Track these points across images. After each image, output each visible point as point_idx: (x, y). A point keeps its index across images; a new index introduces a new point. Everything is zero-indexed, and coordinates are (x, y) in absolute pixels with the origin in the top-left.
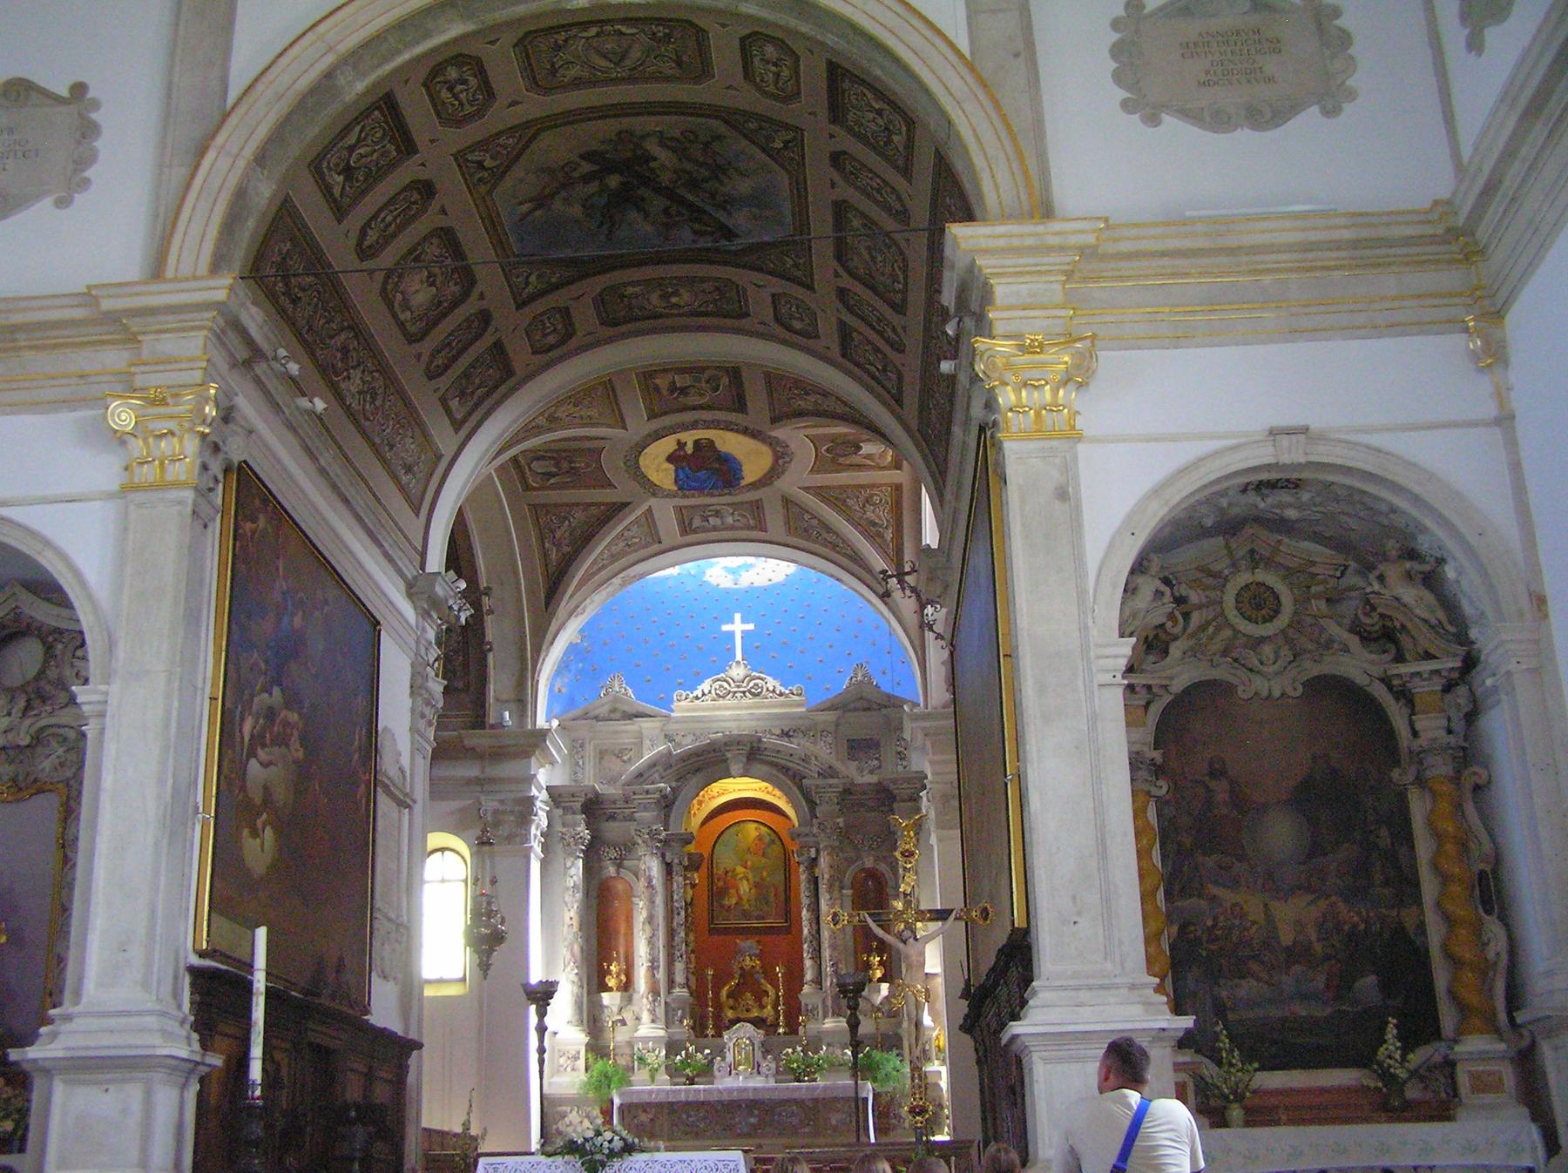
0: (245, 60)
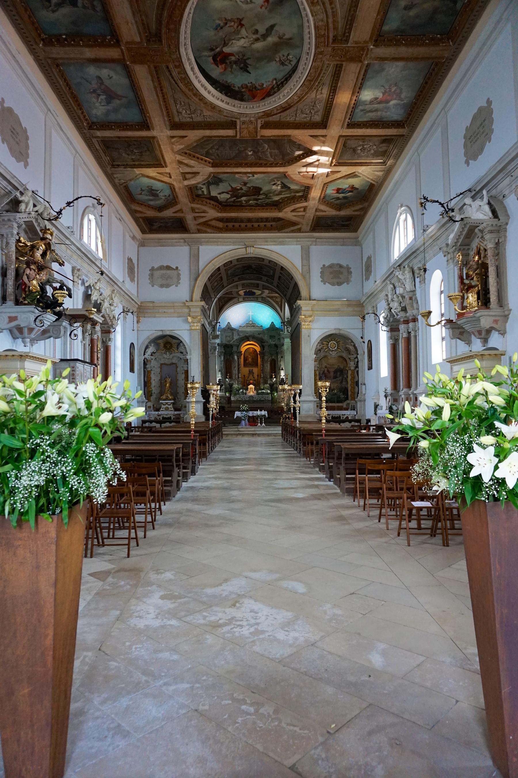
0: (201, 266)
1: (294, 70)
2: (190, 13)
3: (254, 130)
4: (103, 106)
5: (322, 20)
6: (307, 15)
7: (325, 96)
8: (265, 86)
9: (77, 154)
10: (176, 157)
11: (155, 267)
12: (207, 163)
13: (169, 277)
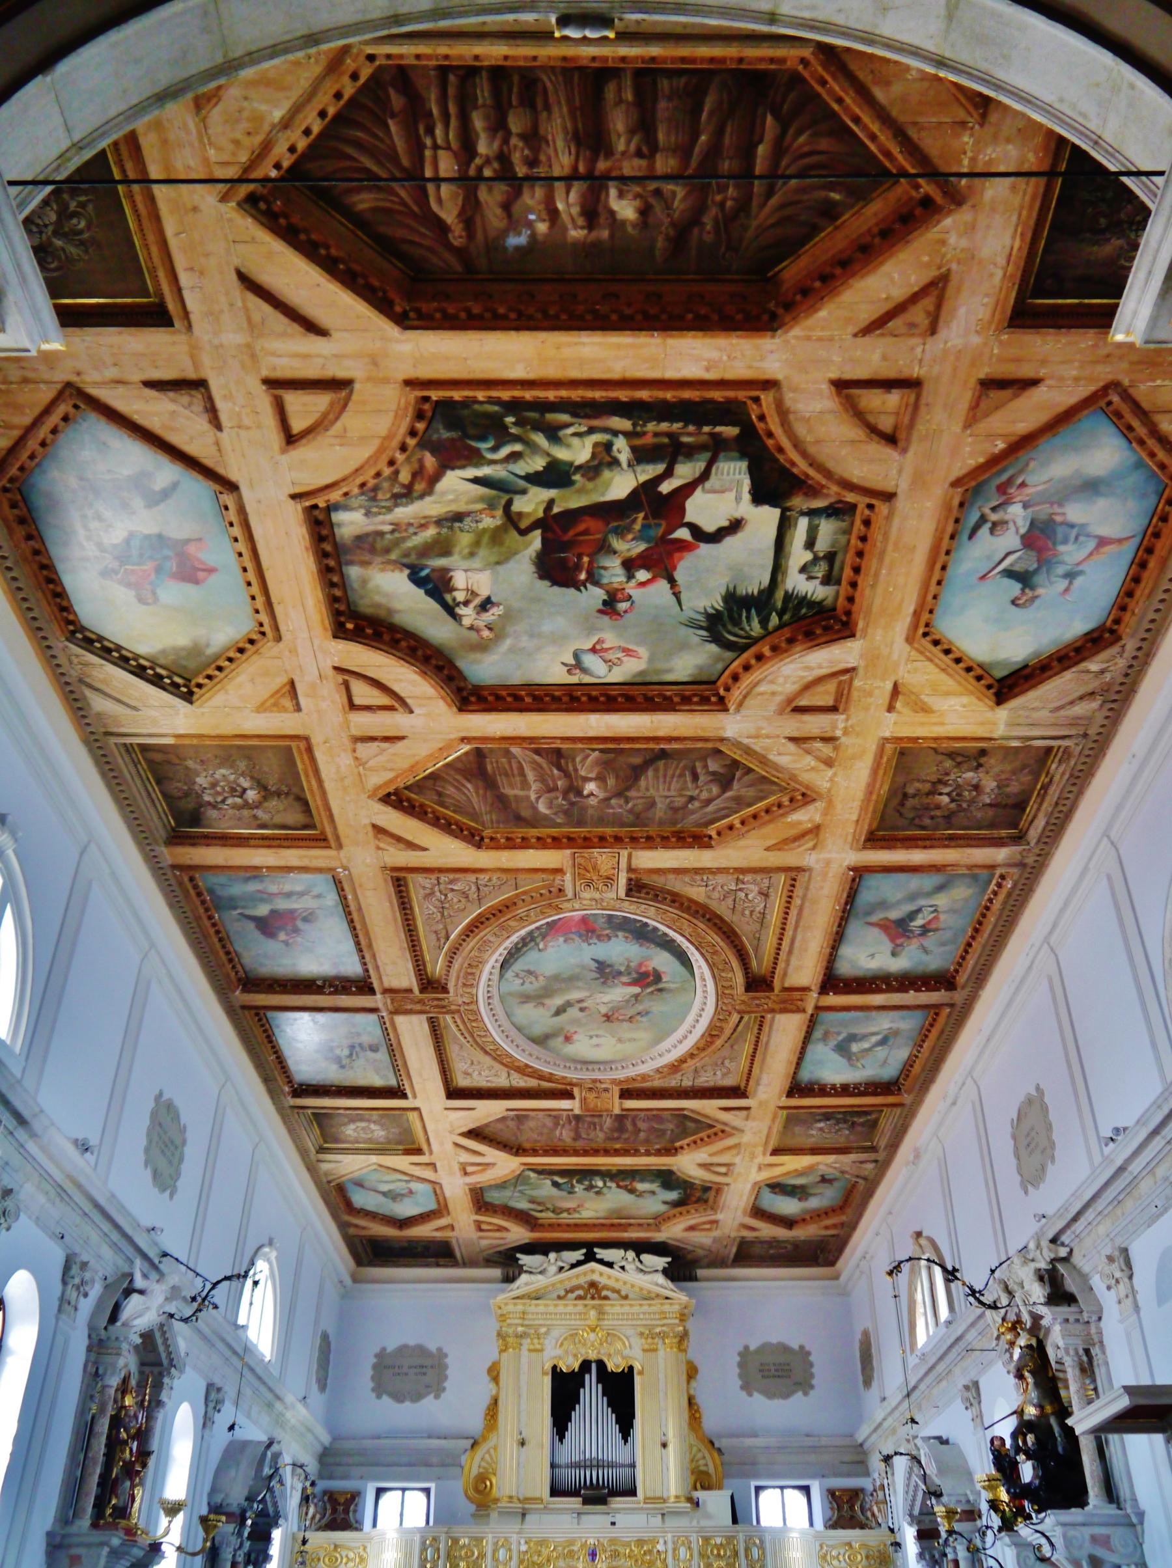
1: (504, 965)
8: (561, 939)
10: (831, 780)
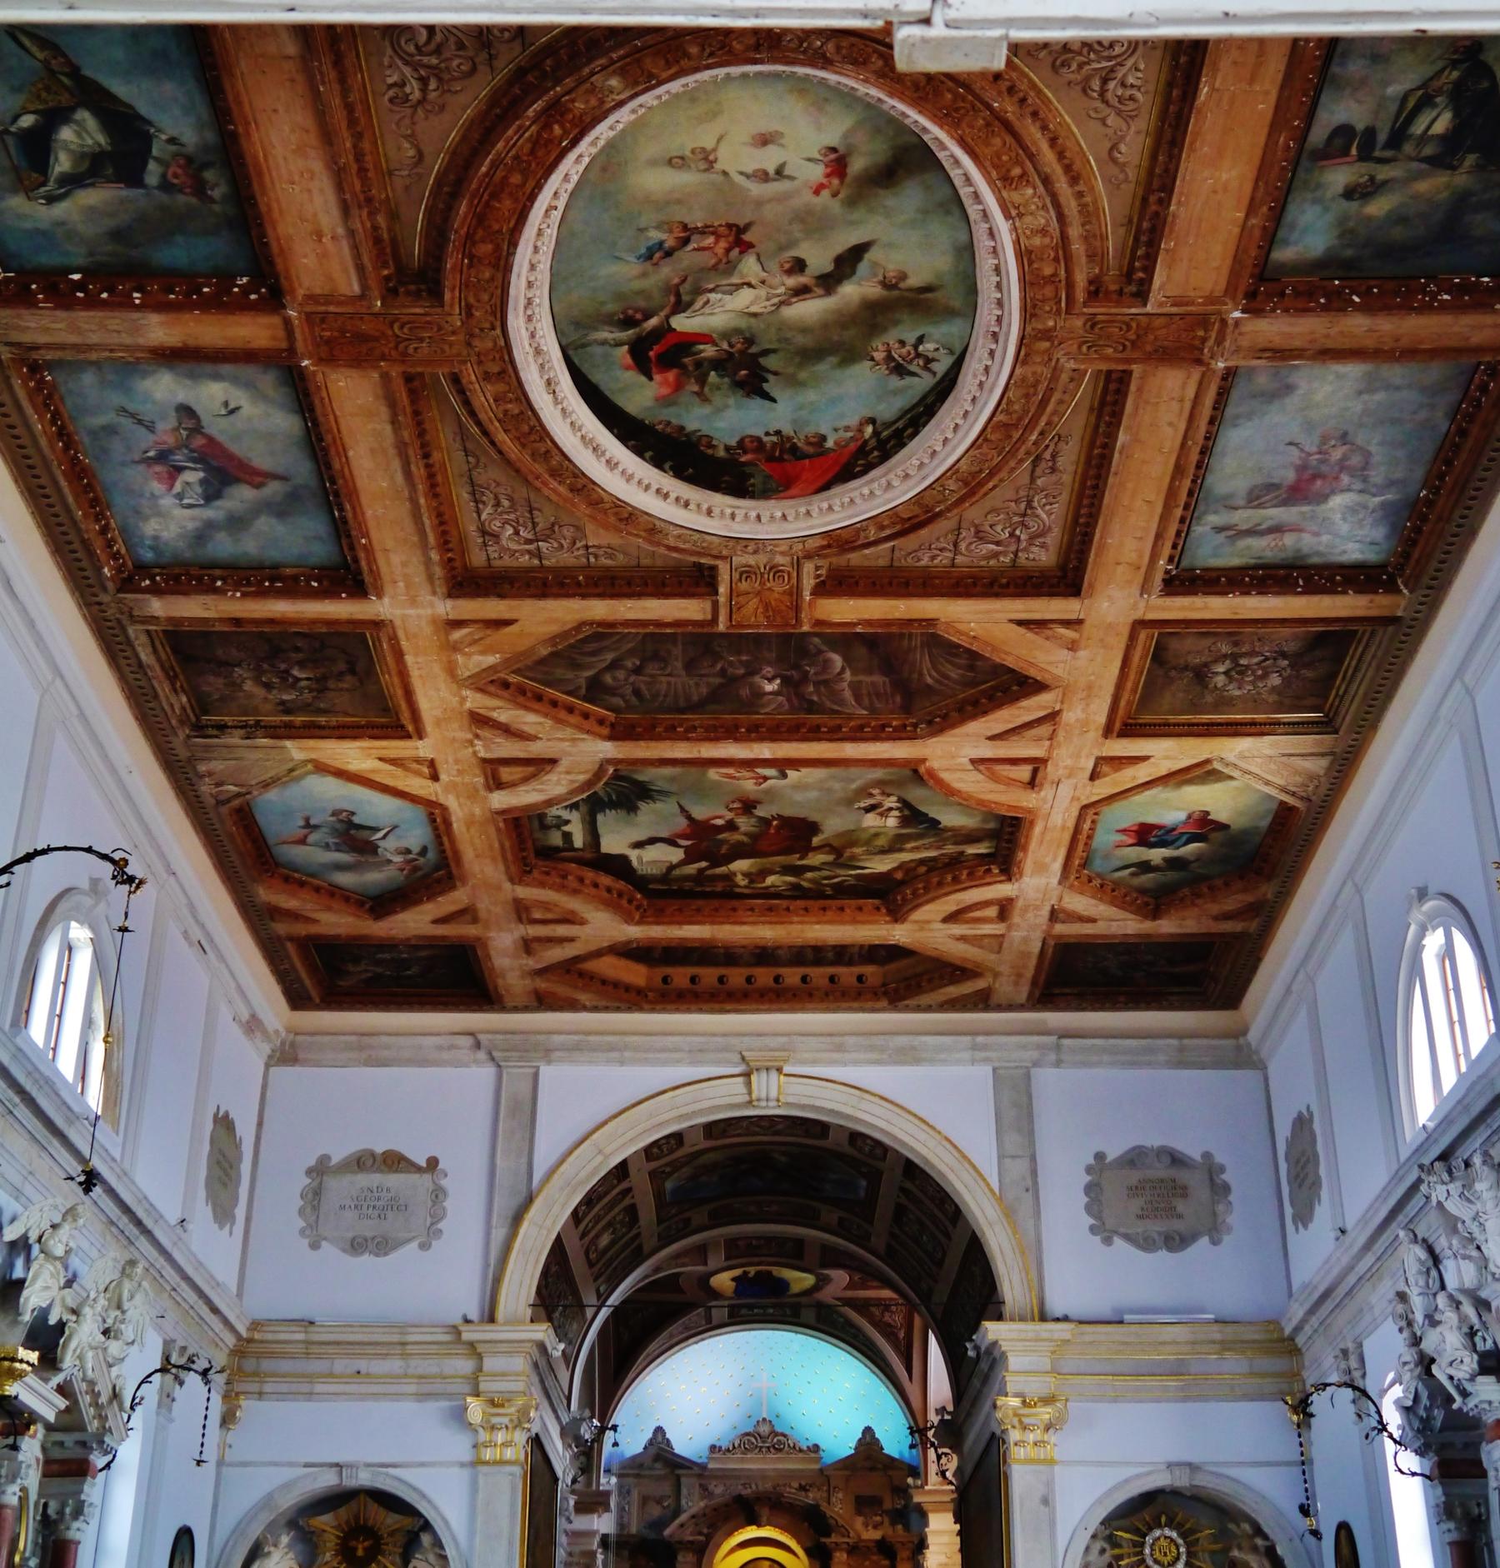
0: (544, 1157)
1: (946, 386)
2: (556, 208)
3: (786, 598)
4: (190, 506)
5: (1043, 232)
6: (985, 215)
7: (1067, 478)
8: (830, 444)
9: (58, 682)
10: (463, 700)
11: (335, 1160)
12: (591, 724)
13: (397, 1205)
